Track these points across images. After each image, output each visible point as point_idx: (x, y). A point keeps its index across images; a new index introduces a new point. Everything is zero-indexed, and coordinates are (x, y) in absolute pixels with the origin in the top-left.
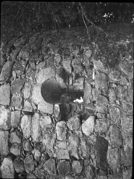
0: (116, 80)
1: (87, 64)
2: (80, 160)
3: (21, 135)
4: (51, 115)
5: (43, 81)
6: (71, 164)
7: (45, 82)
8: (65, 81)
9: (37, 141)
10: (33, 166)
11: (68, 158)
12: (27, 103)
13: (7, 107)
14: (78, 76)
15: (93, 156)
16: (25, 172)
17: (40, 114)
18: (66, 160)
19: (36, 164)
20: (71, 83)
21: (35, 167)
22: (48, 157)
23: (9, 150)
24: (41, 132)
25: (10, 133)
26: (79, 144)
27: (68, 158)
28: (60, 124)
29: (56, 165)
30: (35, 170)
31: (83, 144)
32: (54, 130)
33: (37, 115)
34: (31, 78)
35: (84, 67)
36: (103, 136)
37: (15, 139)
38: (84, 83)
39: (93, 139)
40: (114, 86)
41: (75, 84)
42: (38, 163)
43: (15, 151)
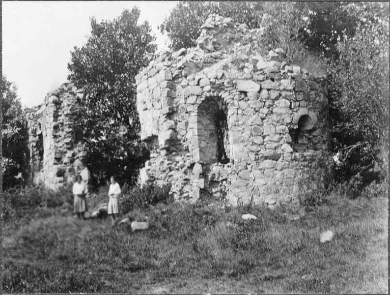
0: (313, 166)
1: (318, 146)
2: (264, 142)
3: (277, 99)
4: (292, 122)
5: (310, 116)
6: (260, 135)
7: (310, 117)
8: (308, 130)
9: (274, 111)
10: (254, 107)
11: (264, 134)
12: (297, 104)
13: (294, 89)
14: (309, 139)
15: (267, 151)
16: (249, 100)
17: (291, 114)
18: (263, 133)
19: (257, 110)
20: (306, 134)
21: (255, 109)
22: (263, 119)
23: (265, 89)
24: (281, 114)
25: (278, 90)
26: (275, 142)
27: (264, 134)
28: (287, 129)
29: (258, 125)
30: (252, 108)
31: (276, 145)
32: (282, 124)
33: (290, 112)
34: (311, 106)
35: (315, 144)
36: (282, 158)
37: (274, 94)
38: (305, 144)
39: (279, 151)
40: (310, 165)
41: (304, 138)
42: (257, 111)
43: (264, 93)
